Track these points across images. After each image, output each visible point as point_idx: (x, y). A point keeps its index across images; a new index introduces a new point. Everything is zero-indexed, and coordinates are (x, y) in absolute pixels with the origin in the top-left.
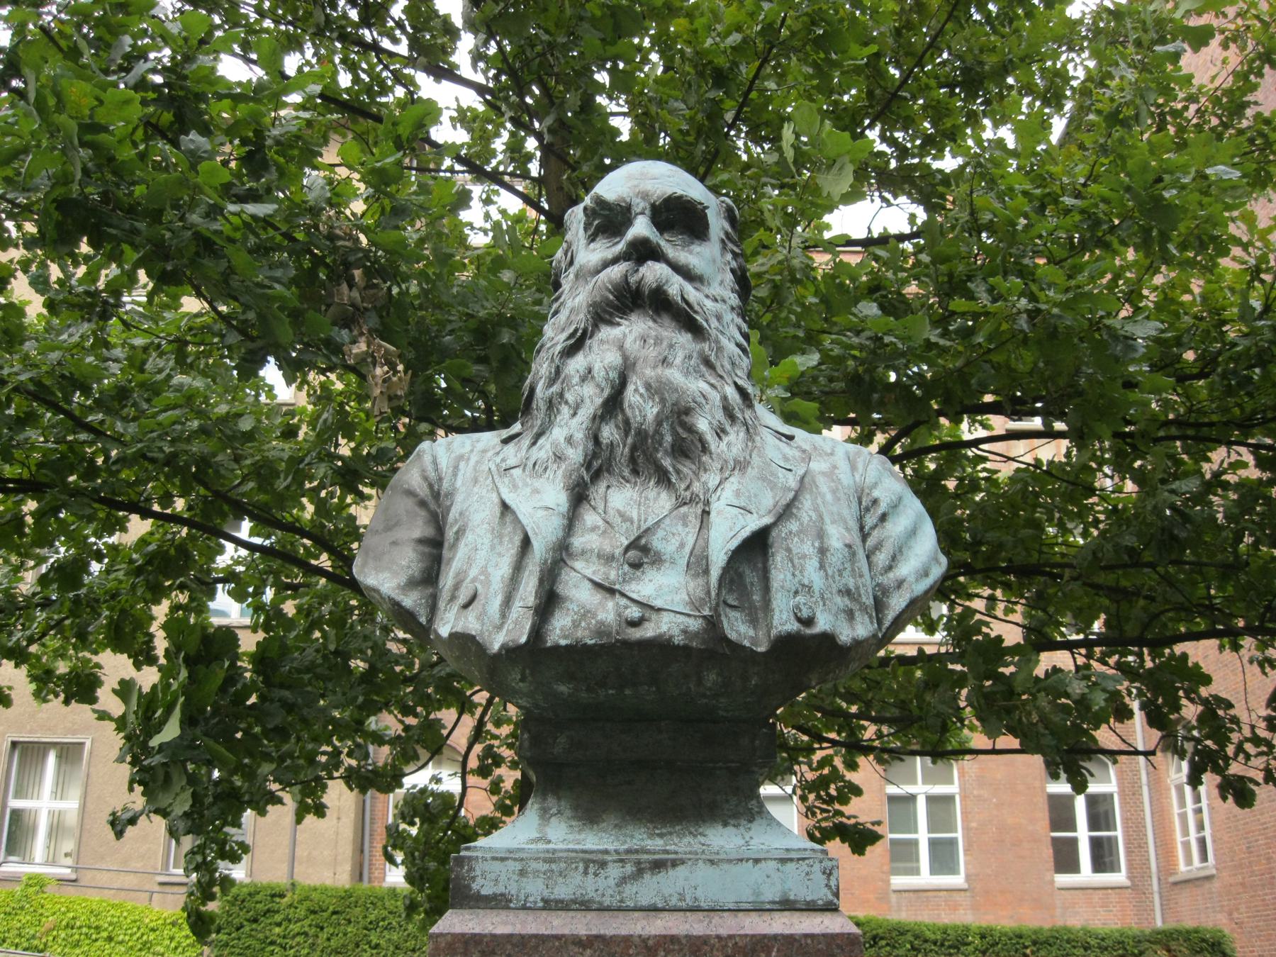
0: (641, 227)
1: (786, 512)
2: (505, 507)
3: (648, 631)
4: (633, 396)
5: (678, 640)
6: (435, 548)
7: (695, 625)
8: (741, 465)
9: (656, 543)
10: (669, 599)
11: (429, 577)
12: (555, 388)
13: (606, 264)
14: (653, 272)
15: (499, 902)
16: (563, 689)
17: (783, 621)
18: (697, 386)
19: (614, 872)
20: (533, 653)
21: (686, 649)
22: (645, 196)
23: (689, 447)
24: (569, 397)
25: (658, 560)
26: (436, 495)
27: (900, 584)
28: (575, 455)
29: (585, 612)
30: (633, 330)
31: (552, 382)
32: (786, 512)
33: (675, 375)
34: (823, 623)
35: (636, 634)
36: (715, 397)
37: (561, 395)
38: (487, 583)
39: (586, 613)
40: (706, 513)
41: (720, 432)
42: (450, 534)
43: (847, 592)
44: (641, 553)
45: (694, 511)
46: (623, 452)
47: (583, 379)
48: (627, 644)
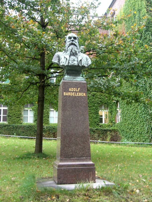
0: (72, 39)
1: (82, 58)
2: (64, 57)
3: (75, 65)
4: (73, 50)
8: (80, 55)
9: (75, 60)
10: (76, 63)
11: (59, 61)
14: (74, 42)
15: (66, 80)
16: (69, 68)
17: (82, 65)
18: (77, 50)
19: (72, 79)
20: (68, 66)
21: (77, 66)
23: (76, 54)
25: (75, 61)
27: (89, 64)
28: (69, 54)
29: (71, 63)
30: (72, 46)
31: (67, 49)
32: (82, 58)
33: (75, 49)
34: (85, 65)
35: (74, 65)
36: (78, 51)
40: (78, 58)
41: (78, 53)
42: (60, 59)
44: (74, 60)
45: (77, 58)
46: (72, 54)
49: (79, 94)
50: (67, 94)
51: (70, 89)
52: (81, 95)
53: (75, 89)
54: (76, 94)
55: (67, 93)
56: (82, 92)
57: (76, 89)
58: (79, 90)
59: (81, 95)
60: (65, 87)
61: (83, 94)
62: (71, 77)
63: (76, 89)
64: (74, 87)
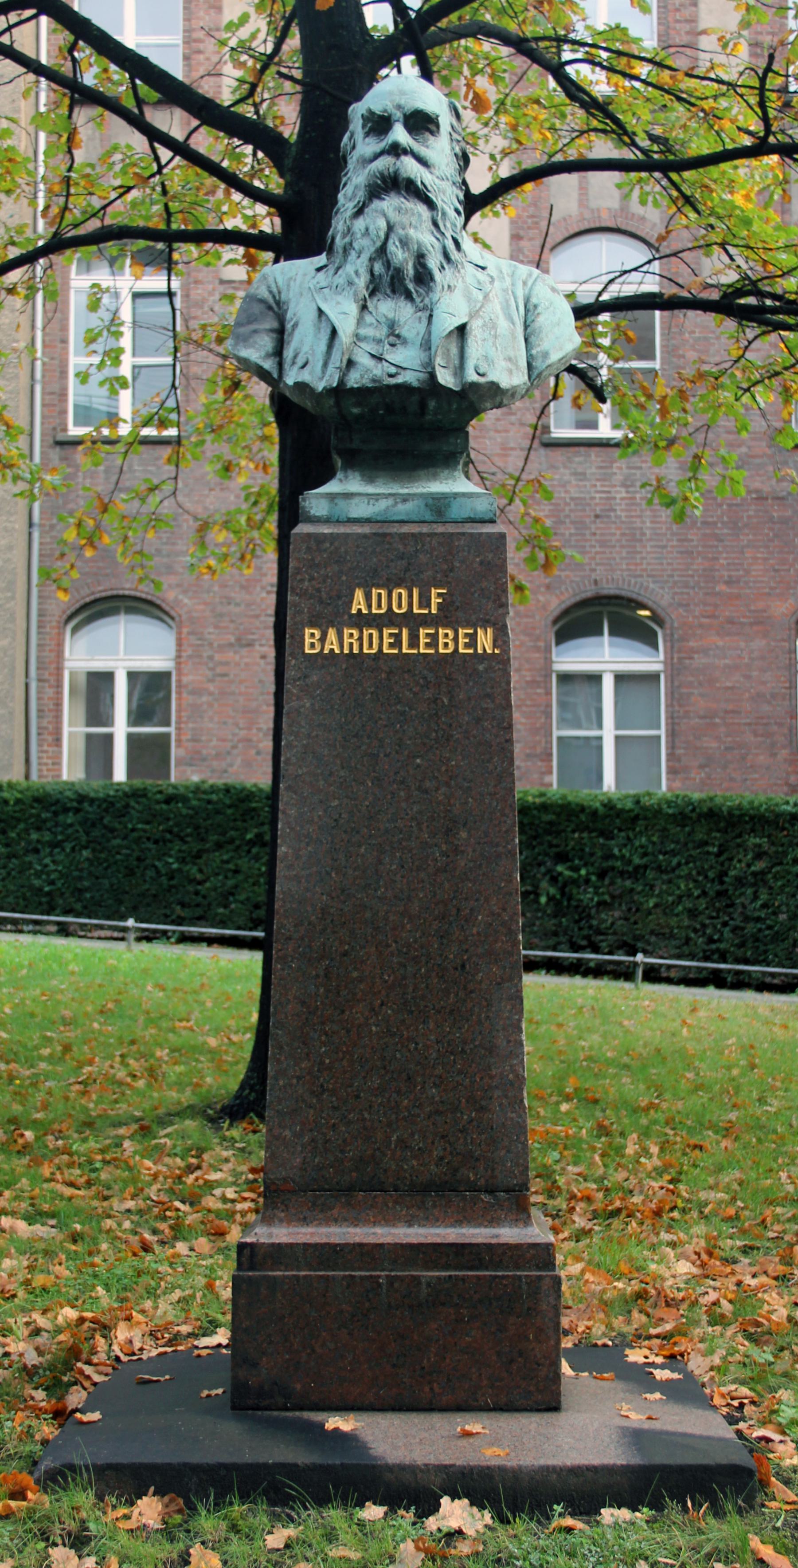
2: (321, 312)
3: (400, 380)
5: (415, 384)
6: (281, 335)
7: (422, 376)
11: (278, 352)
12: (347, 240)
13: (376, 156)
22: (399, 107)
23: (424, 277)
24: (356, 245)
25: (405, 342)
26: (278, 303)
30: (390, 204)
31: (344, 236)
35: (393, 381)
37: (351, 244)
38: (313, 354)
39: (368, 370)
40: (431, 316)
42: (289, 326)
43: (510, 359)
45: (424, 315)
46: (386, 279)
47: (363, 235)
48: (388, 387)
49: (434, 637)
50: (332, 643)
51: (359, 595)
52: (456, 650)
53: (401, 600)
54: (414, 641)
55: (332, 634)
56: (468, 625)
57: (415, 592)
58: (435, 601)
59: (456, 650)
60: (312, 579)
61: (473, 640)
62: (370, 489)
63: (415, 592)
64: (390, 585)
